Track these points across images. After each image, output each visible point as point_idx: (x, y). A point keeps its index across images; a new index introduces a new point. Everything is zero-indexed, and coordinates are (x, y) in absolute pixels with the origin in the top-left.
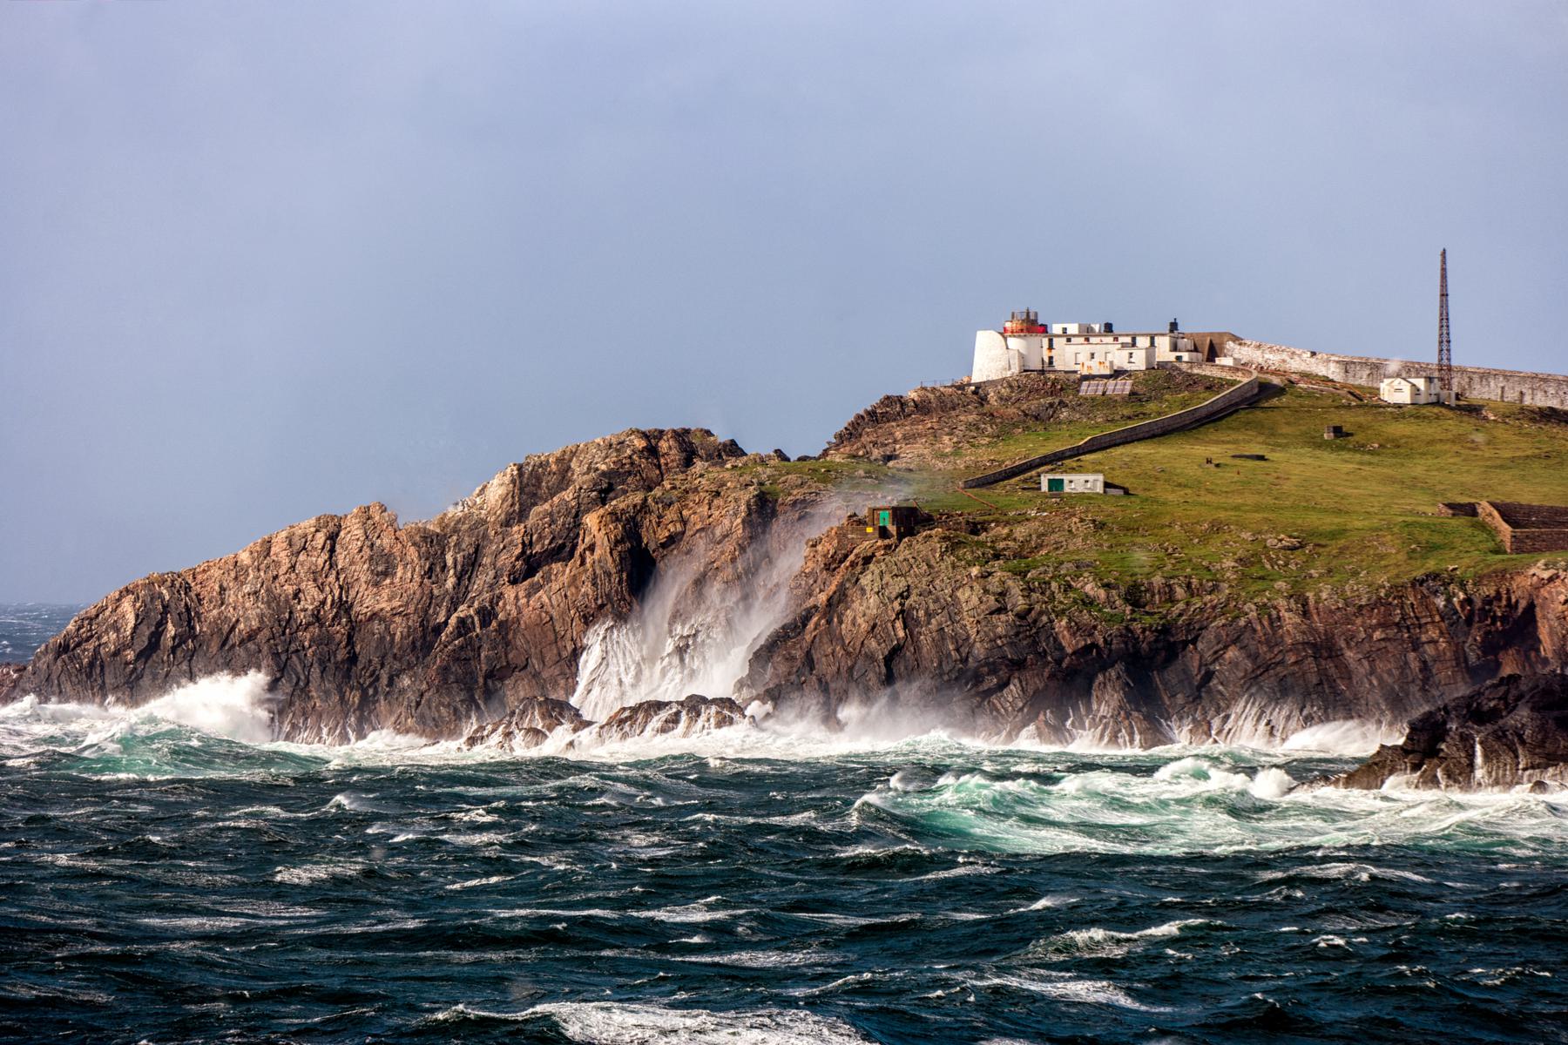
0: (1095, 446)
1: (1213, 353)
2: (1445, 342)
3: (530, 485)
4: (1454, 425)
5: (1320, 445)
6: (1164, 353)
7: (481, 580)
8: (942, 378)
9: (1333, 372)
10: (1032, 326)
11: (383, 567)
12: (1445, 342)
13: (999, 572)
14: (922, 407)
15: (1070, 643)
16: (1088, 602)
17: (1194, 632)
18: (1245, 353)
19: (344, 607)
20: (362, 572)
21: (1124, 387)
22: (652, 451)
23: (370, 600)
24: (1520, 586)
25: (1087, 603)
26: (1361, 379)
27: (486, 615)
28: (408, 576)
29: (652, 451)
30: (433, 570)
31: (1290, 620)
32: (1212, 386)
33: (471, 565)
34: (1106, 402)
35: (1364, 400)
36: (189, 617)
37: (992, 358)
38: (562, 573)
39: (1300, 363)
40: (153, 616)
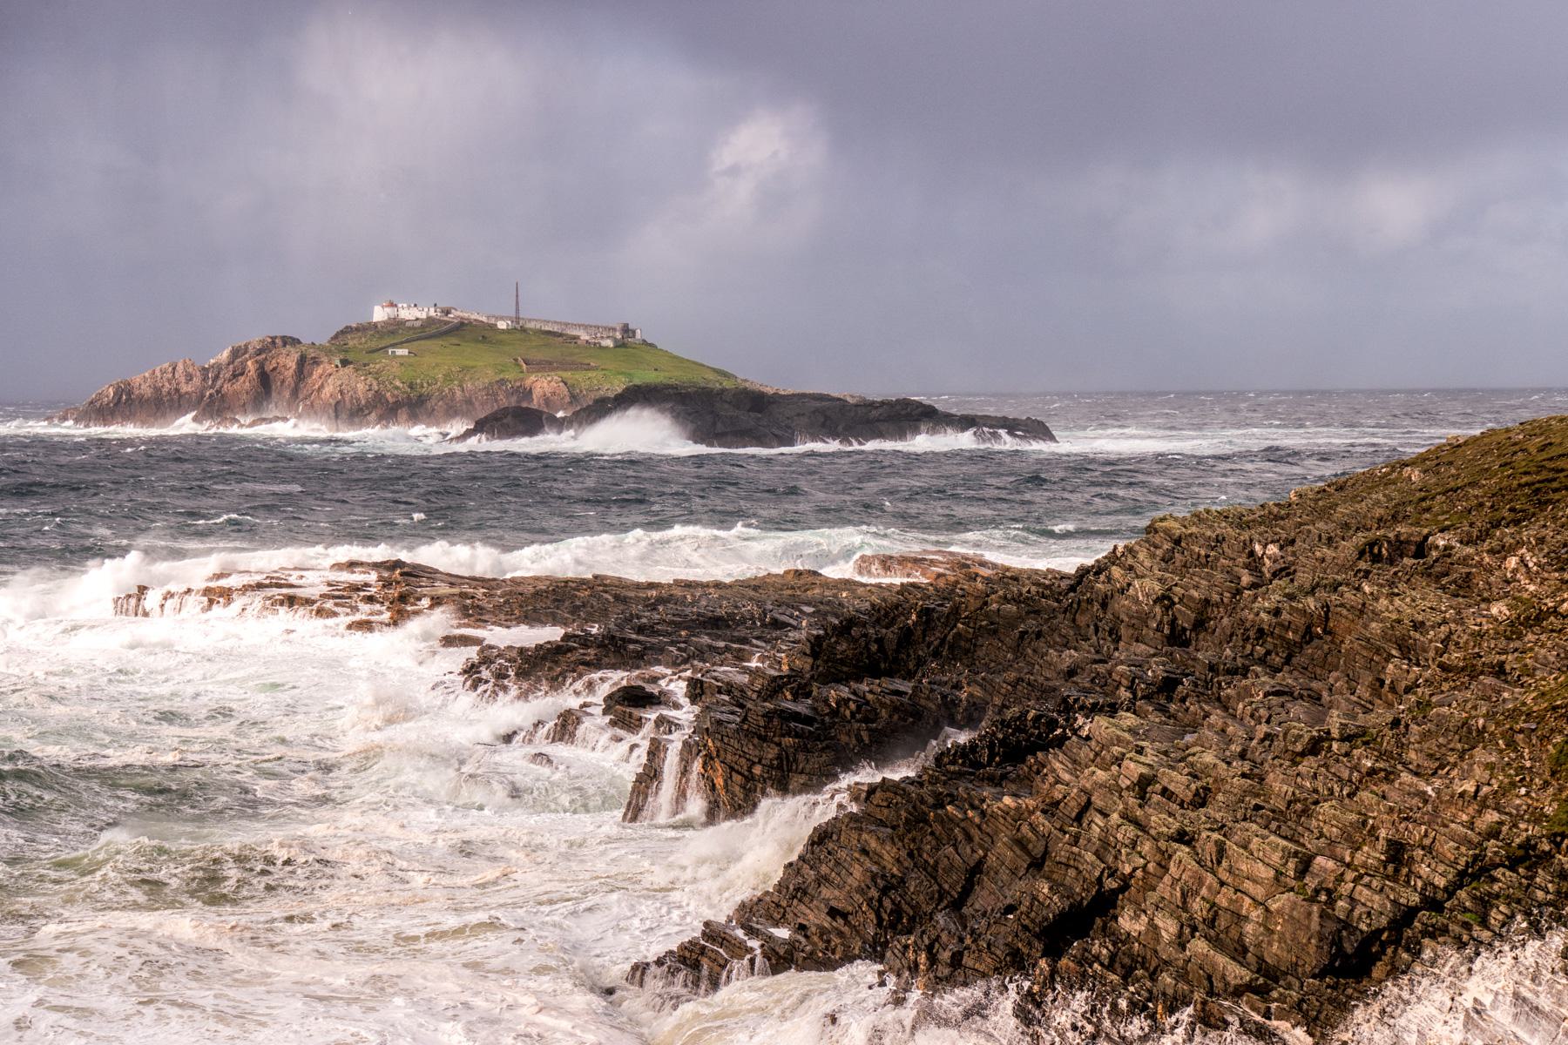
0: (407, 341)
1: (448, 312)
2: (517, 310)
3: (236, 353)
4: (518, 335)
5: (477, 341)
6: (432, 313)
7: (219, 383)
8: (364, 321)
9: (484, 319)
10: (392, 305)
11: (189, 378)
12: (517, 310)
13: (370, 378)
14: (357, 329)
15: (391, 400)
16: (397, 388)
17: (429, 397)
18: (458, 313)
19: (177, 390)
20: (183, 379)
21: (418, 324)
22: (273, 343)
23: (185, 388)
24: (528, 383)
25: (397, 386)
26: (492, 321)
27: (218, 392)
28: (197, 381)
29: (273, 343)
30: (205, 379)
31: (458, 393)
32: (446, 323)
33: (216, 378)
34: (413, 328)
35: (493, 327)
36: (129, 393)
37: (380, 314)
38: (242, 379)
39: (474, 316)
40: (119, 392)
